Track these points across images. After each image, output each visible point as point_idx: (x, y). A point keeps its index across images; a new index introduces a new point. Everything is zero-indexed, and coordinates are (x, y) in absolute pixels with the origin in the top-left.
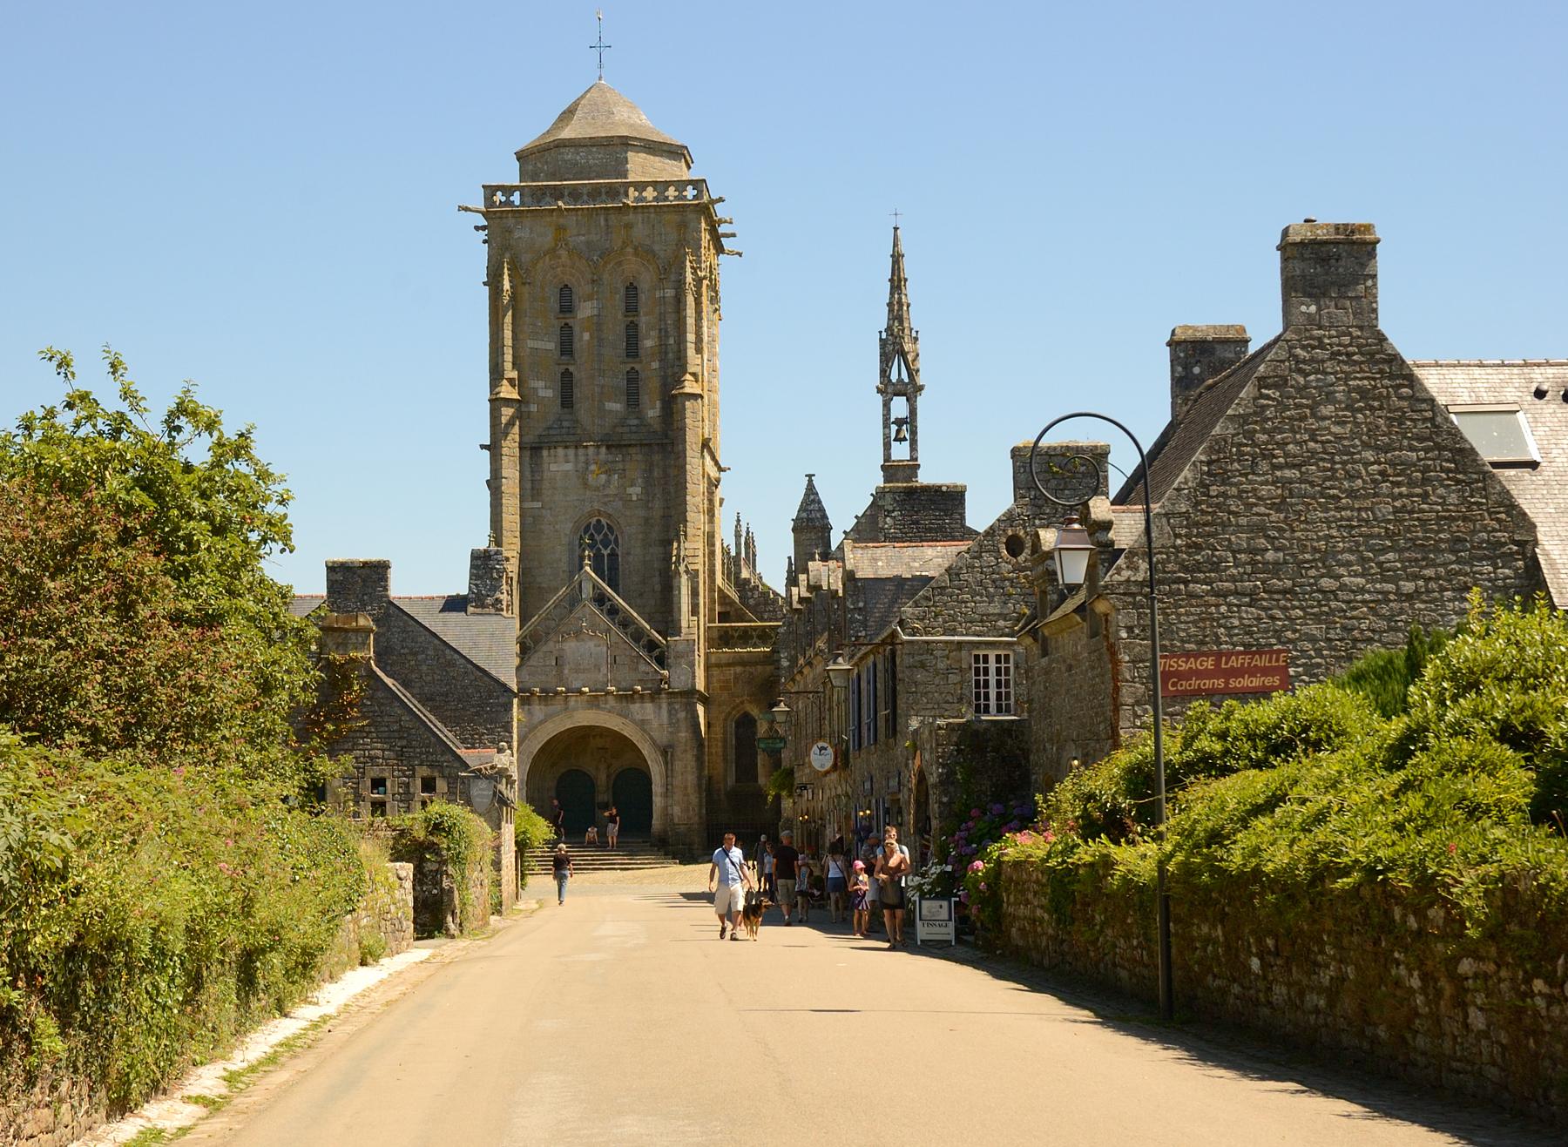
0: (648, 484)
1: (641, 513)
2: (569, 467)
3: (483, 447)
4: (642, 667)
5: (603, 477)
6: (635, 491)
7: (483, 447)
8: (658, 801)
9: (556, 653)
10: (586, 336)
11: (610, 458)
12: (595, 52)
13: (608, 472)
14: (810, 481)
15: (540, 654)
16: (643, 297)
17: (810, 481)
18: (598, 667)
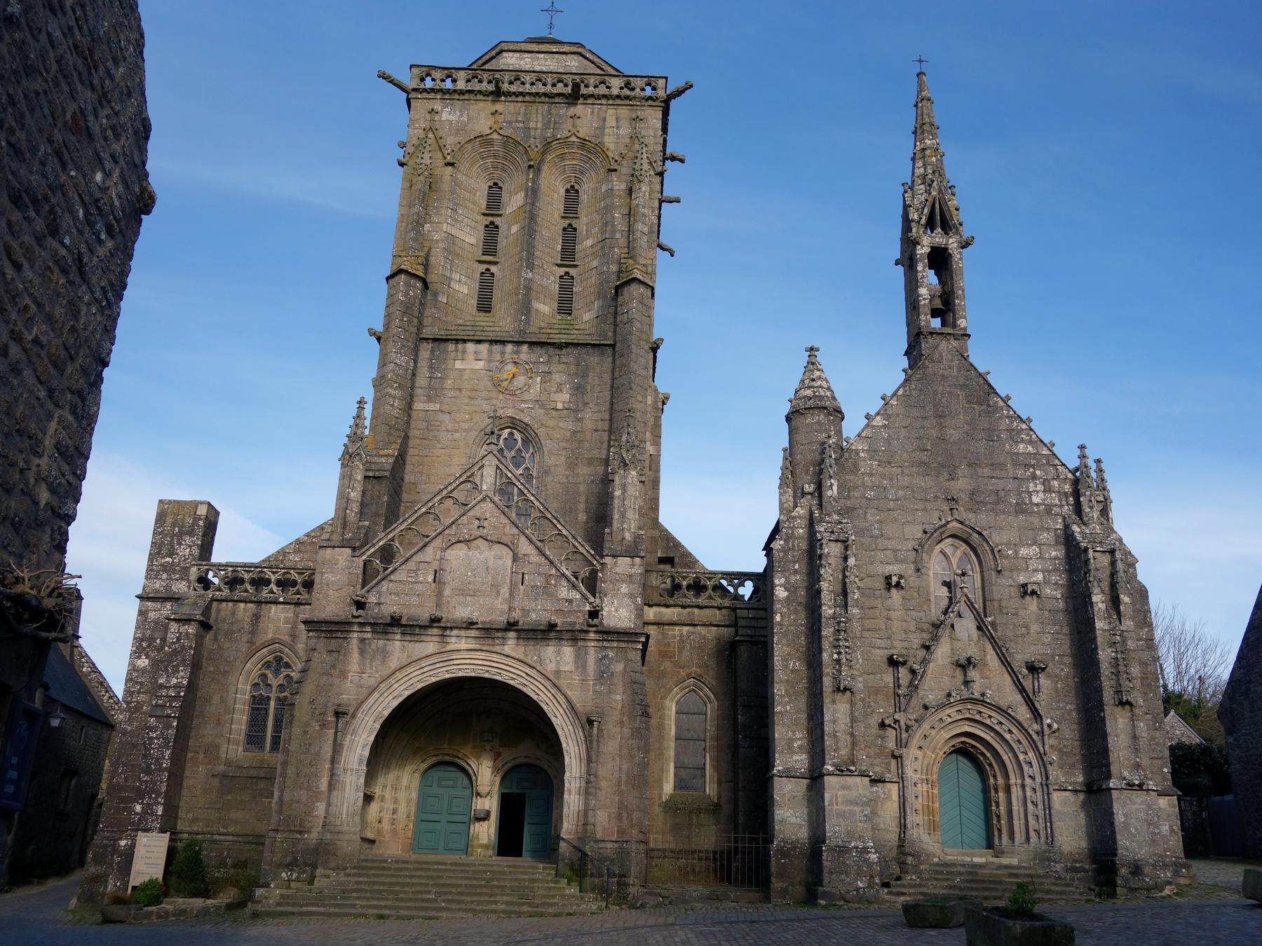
0: (579, 390)
1: (570, 425)
2: (481, 364)
3: (372, 333)
4: (564, 592)
5: (521, 380)
6: (562, 399)
7: (372, 333)
8: (572, 801)
9: (436, 565)
10: (515, 229)
11: (533, 358)
12: (547, 16)
13: (530, 373)
14: (812, 364)
15: (411, 565)
16: (584, 197)
17: (812, 364)
18: (496, 587)
